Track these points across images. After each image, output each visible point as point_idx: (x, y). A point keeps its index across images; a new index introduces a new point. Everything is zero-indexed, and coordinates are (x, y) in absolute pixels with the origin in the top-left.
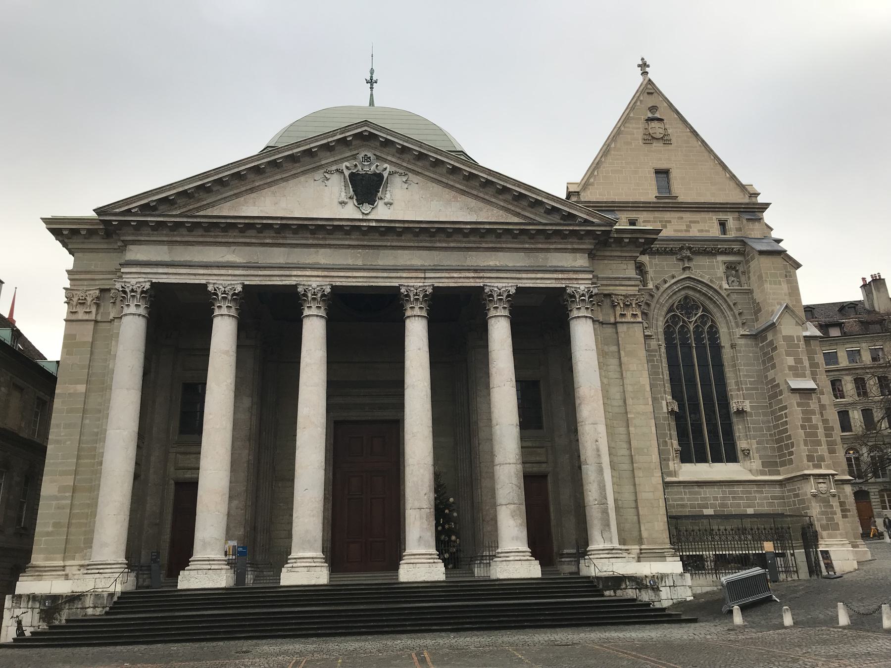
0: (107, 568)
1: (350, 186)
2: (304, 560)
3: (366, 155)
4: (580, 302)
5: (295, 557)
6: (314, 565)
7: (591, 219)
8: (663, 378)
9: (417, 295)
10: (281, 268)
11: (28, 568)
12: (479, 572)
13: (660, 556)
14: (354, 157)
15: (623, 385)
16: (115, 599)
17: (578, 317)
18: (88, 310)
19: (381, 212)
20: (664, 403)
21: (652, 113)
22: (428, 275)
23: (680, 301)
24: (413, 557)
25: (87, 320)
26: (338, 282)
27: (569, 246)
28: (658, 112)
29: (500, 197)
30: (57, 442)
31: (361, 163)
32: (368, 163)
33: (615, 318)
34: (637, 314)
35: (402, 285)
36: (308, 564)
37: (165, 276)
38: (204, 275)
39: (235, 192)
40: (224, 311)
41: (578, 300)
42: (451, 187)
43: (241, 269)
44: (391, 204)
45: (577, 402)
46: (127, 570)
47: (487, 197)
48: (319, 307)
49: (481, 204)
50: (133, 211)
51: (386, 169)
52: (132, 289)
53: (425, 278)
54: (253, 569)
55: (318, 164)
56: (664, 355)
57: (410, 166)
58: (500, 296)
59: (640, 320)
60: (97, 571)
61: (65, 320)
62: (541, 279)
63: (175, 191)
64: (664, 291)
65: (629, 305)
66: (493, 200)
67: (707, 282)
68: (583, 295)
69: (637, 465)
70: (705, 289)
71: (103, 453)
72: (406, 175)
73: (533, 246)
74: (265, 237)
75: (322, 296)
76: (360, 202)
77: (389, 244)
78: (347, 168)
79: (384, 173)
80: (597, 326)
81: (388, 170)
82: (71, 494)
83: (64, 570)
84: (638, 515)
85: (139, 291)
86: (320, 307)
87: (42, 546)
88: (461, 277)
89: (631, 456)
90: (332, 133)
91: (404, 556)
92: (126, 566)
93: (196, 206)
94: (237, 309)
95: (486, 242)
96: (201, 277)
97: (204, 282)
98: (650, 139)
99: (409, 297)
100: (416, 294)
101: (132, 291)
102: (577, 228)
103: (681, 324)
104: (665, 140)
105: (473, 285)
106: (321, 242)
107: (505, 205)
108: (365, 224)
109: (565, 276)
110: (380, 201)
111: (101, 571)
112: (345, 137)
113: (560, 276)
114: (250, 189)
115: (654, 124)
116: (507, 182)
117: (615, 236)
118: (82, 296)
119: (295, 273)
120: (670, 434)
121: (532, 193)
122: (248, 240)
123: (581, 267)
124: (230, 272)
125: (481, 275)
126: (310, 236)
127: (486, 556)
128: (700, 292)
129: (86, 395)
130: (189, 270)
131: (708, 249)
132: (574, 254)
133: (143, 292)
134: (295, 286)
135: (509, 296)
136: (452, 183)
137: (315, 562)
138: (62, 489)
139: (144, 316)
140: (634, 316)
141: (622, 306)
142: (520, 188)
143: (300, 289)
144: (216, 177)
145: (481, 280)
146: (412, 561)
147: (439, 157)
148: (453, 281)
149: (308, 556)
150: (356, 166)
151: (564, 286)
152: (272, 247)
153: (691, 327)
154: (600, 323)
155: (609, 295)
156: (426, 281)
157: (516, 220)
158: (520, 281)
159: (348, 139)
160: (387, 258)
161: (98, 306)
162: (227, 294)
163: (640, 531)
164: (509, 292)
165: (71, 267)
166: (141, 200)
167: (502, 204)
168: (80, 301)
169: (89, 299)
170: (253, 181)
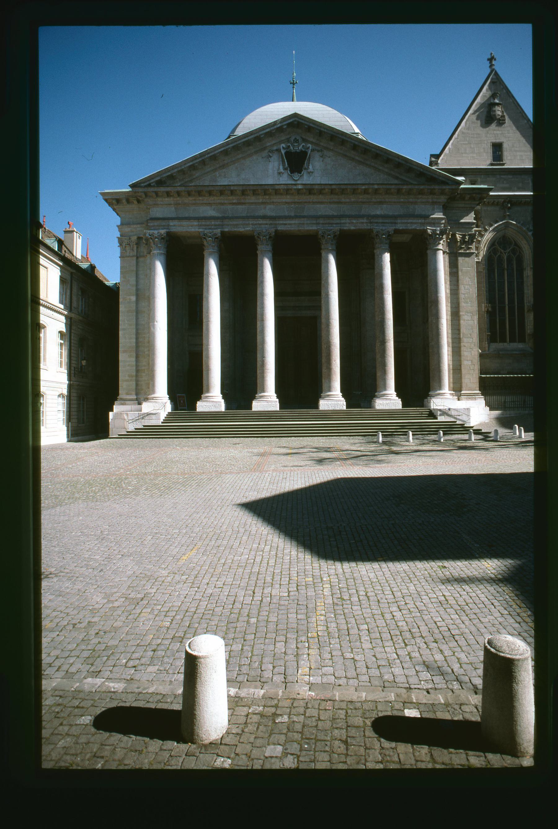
10: (243, 218)
13: (471, 396)
14: (288, 140)
19: (305, 179)
23: (500, 239)
26: (280, 228)
30: (124, 329)
42: (353, 159)
43: (219, 220)
44: (312, 173)
51: (309, 147)
62: (412, 223)
63: (176, 170)
66: (381, 168)
72: (322, 151)
76: (292, 172)
81: (310, 148)
83: (137, 400)
103: (499, 254)
112: (281, 127)
135: (389, 235)
157: (396, 182)
165: (119, 223)
170: (224, 160)
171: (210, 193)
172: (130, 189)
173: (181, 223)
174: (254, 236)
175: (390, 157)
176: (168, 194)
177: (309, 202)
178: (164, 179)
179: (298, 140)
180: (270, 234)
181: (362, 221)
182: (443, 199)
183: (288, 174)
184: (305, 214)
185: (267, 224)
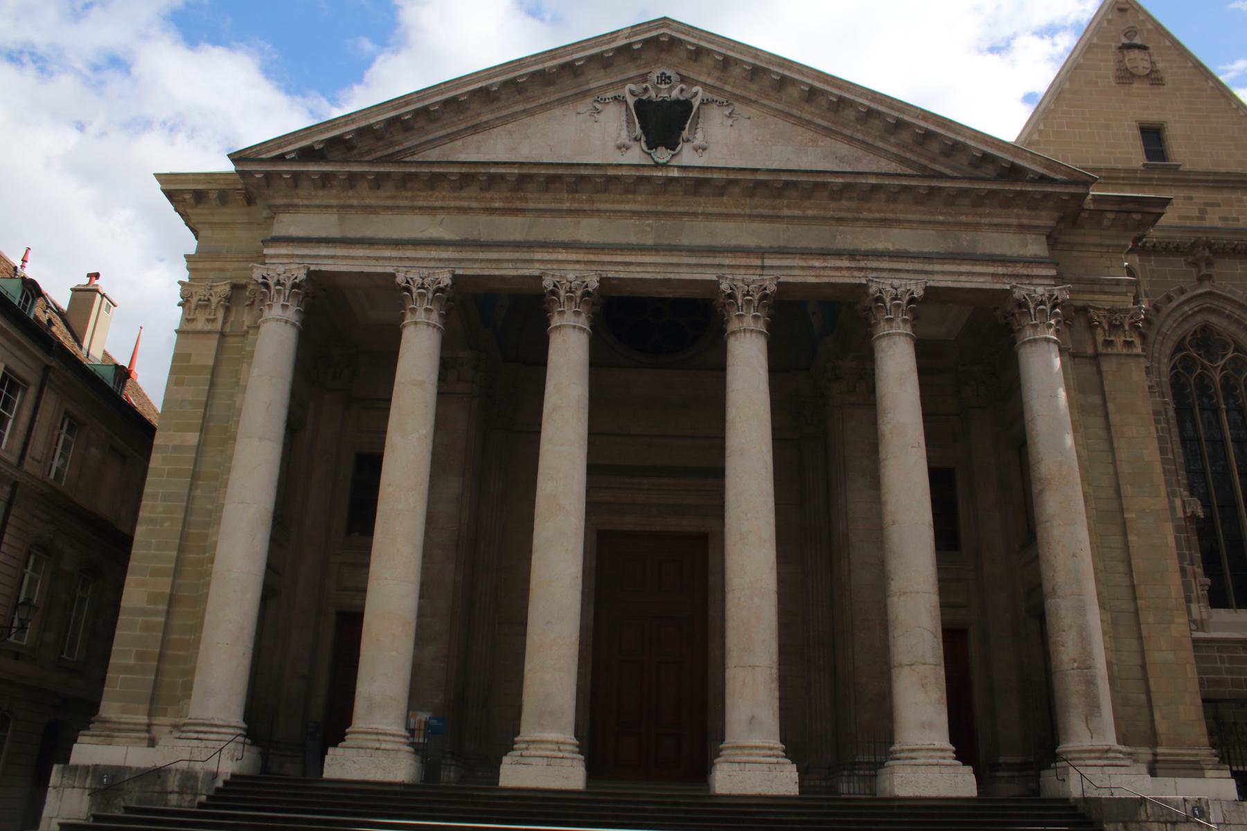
0: (212, 733)
1: (636, 120)
2: (543, 746)
3: (663, 74)
4: (1037, 315)
5: (527, 738)
6: (560, 754)
7: (1052, 175)
8: (1175, 459)
9: (748, 295)
11: (93, 723)
12: (849, 788)
15: (1114, 460)
16: (220, 784)
17: (1035, 340)
18: (212, 317)
20: (1178, 502)
21: (1128, 38)
22: (768, 262)
23: (1195, 332)
24: (738, 751)
25: (209, 332)
27: (1014, 221)
28: (1138, 37)
29: (893, 140)
31: (654, 87)
32: (668, 86)
33: (1095, 346)
34: (1133, 342)
35: (722, 277)
36: (549, 753)
37: (330, 261)
38: (390, 259)
39: (449, 130)
40: (421, 315)
41: (1032, 311)
42: (807, 124)
43: (451, 249)
44: (704, 149)
45: (1036, 488)
46: (241, 739)
47: (868, 140)
48: (577, 313)
49: (860, 153)
50: (288, 157)
51: (696, 94)
52: (279, 281)
53: (763, 267)
54: (453, 762)
55: (586, 88)
56: (1173, 422)
57: (738, 92)
58: (896, 299)
59: (1138, 350)
60: (195, 735)
61: (177, 331)
62: (968, 274)
63: (354, 127)
64: (1169, 315)
65: (1119, 325)
67: (1241, 301)
68: (1042, 303)
69: (1143, 602)
70: (1238, 312)
71: (216, 543)
73: (951, 219)
74: (492, 199)
75: (583, 296)
76: (652, 145)
77: (700, 210)
78: (632, 93)
79: (693, 100)
80: (1066, 358)
81: (700, 94)
82: (165, 607)
83: (148, 731)
84: (1148, 693)
85: (289, 284)
86: (579, 312)
87: (118, 689)
88: (824, 268)
89: (1133, 587)
90: (608, 37)
91: (721, 750)
92: (244, 733)
93: (386, 153)
94: (441, 315)
95: (870, 210)
96: (386, 263)
97: (390, 270)
98: (1126, 76)
99: (736, 299)
100: (748, 294)
101: (278, 283)
102: (1029, 188)
103: (1199, 371)
104: (1154, 78)
105: (847, 280)
106: (586, 207)
107: (901, 153)
108: (660, 174)
109: (1009, 270)
110: (685, 144)
111: (201, 736)
112: (628, 47)
113: (1001, 270)
114: (473, 126)
115: (1135, 54)
116: (904, 113)
117: (1092, 207)
118: (205, 296)
119: (538, 256)
120: (1191, 555)
121: (947, 130)
122: (465, 204)
123: (1036, 256)
124: (434, 254)
125: (862, 264)
126: (566, 195)
127: (860, 763)
128: (1228, 317)
129: (199, 449)
130: (368, 251)
131: (1239, 248)
132: (1022, 236)
133: (294, 286)
134: (539, 279)
135: (912, 300)
136: (808, 117)
137: (560, 750)
138: (154, 598)
139: (293, 324)
140: (1129, 344)
141: (1106, 327)
142: (926, 121)
143: (548, 283)
144: (419, 105)
145: (863, 274)
146: (738, 759)
147: (787, 73)
148: (813, 274)
149: (550, 739)
150: (646, 90)
151: (1008, 287)
152: (503, 215)
153: (1217, 378)
154: (1070, 354)
155: (1084, 310)
156: (765, 272)
158: (930, 277)
159: (636, 47)
160: (697, 233)
161: (227, 310)
162: (426, 289)
163: (1152, 720)
164: (912, 293)
166: (302, 140)
167: (895, 150)
168: (200, 303)
169: (214, 300)
170: (479, 114)
171: (434, 181)
172: (229, 167)
173: (351, 251)
174: (544, 295)
175: (906, 118)
176: (325, 180)
177: (695, 214)
178: (321, 146)
179: (669, 78)
180: (587, 286)
181: (839, 263)
182: (1046, 219)
183: (643, 151)
184: (685, 241)
185: (578, 262)
